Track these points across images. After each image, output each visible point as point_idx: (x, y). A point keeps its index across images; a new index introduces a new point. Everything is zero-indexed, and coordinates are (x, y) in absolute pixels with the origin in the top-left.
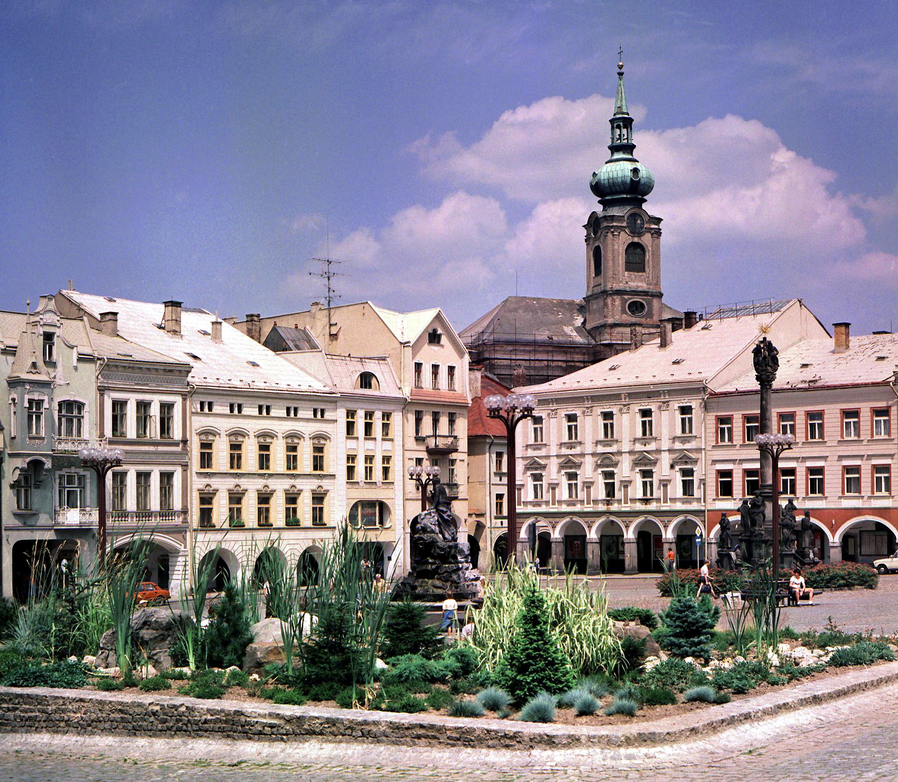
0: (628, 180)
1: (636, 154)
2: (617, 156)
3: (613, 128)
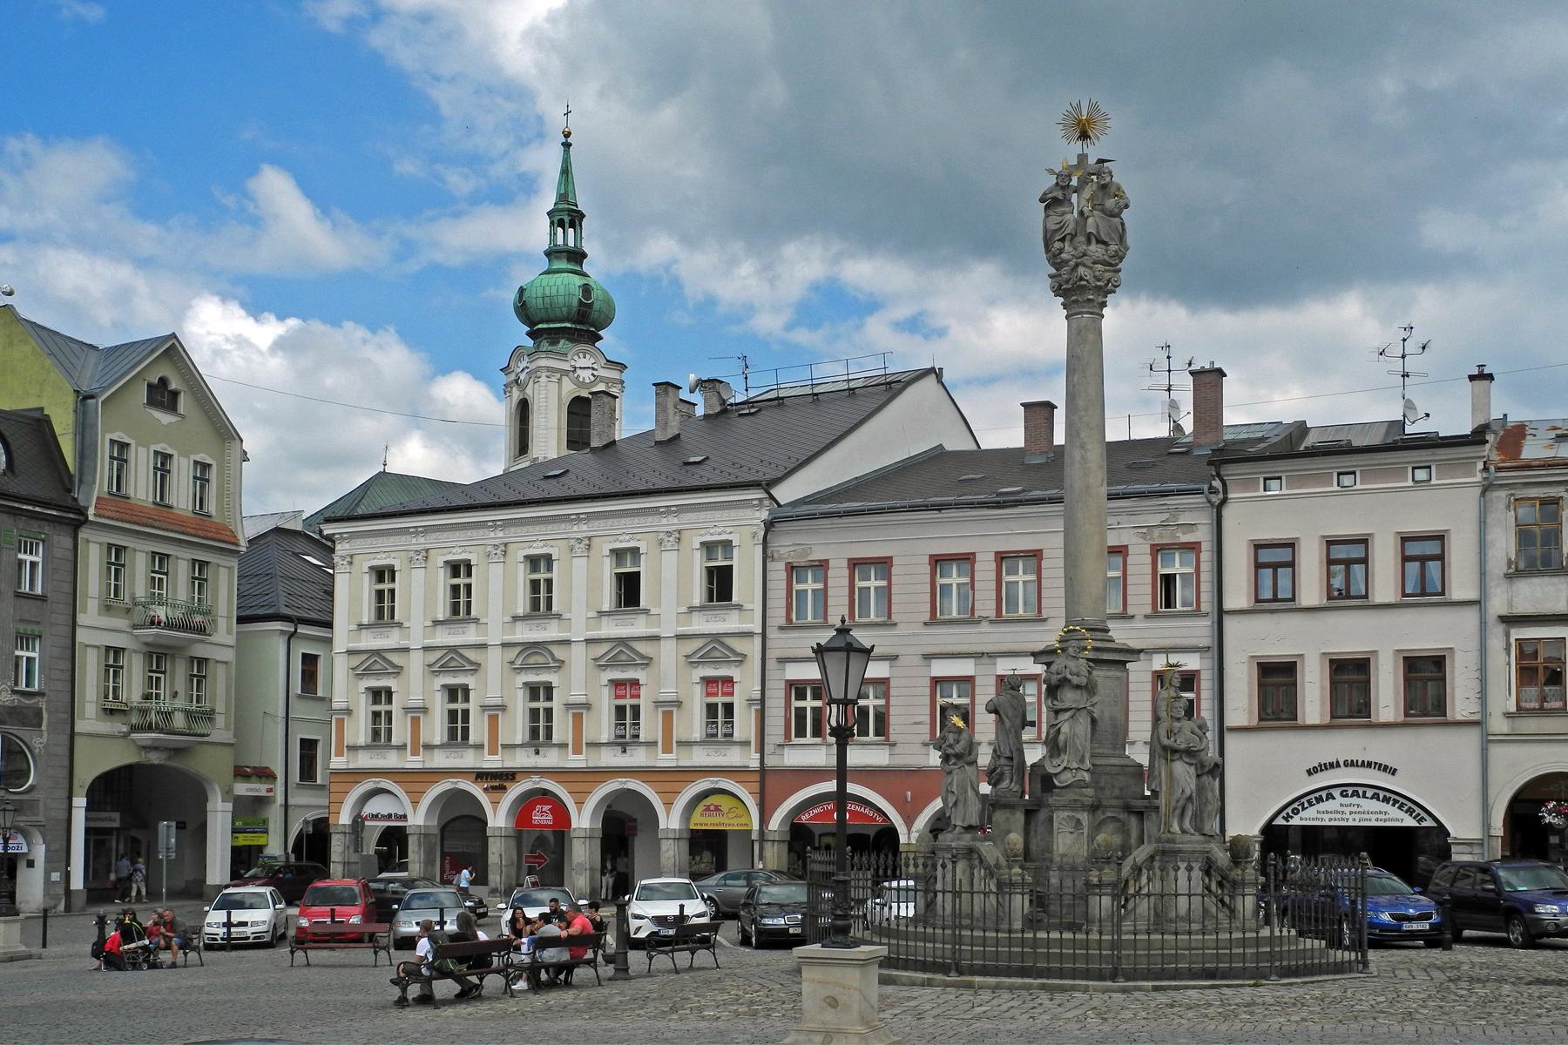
0: (575, 303)
1: (586, 267)
2: (558, 265)
3: (552, 223)
